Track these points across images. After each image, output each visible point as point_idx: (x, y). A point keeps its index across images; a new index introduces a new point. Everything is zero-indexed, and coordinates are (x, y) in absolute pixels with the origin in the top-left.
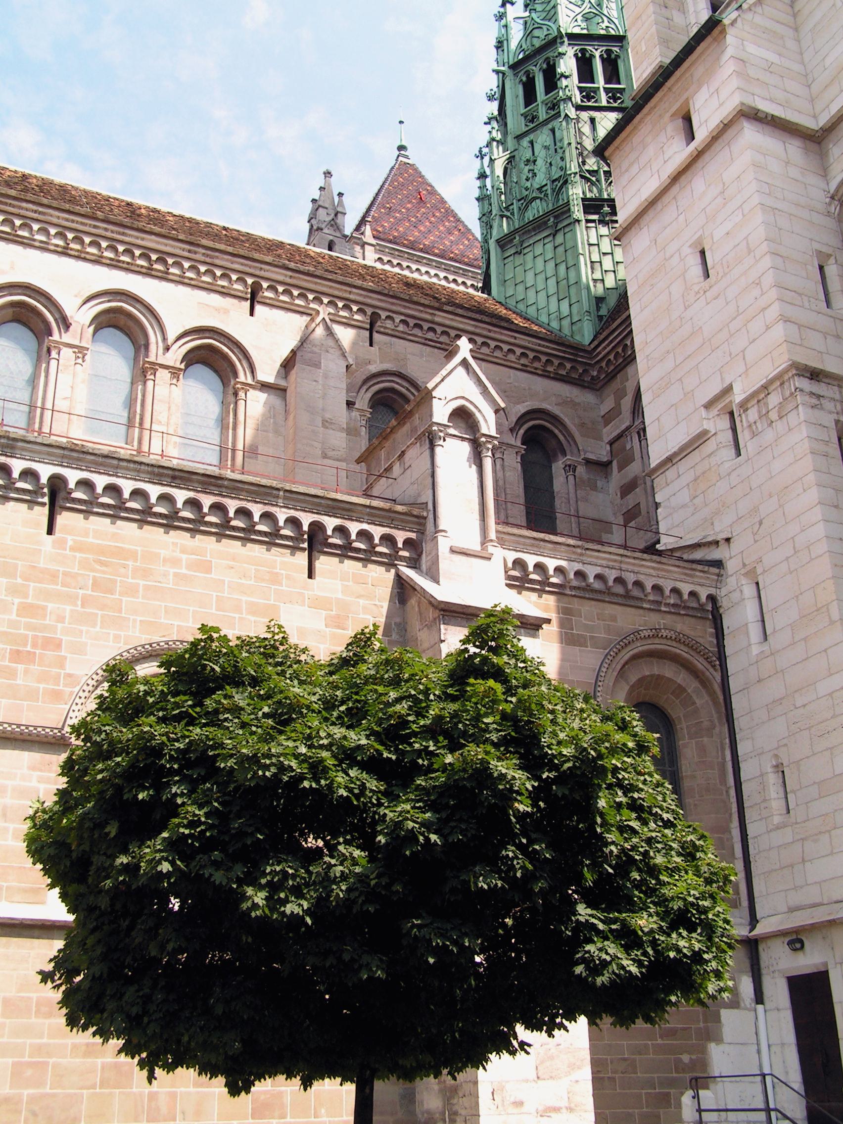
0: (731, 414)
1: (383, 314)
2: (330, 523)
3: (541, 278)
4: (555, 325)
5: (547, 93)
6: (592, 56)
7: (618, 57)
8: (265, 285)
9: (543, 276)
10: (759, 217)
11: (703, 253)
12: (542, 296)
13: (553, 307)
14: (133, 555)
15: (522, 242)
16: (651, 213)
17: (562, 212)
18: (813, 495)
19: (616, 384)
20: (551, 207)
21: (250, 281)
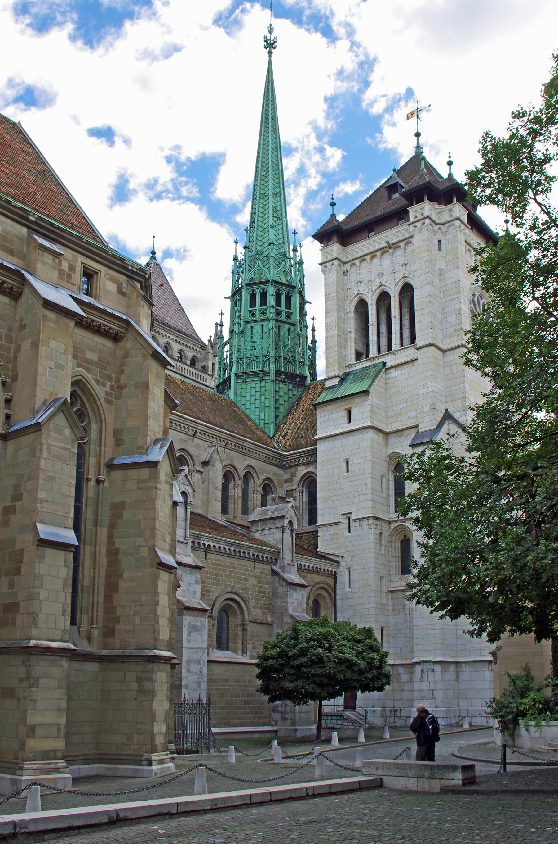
0: (349, 519)
1: (230, 442)
2: (261, 555)
3: (253, 399)
4: (257, 421)
5: (261, 306)
6: (282, 293)
7: (292, 296)
8: (199, 431)
9: (254, 397)
10: (370, 465)
11: (348, 462)
12: (253, 407)
13: (257, 413)
14: (220, 565)
15: (246, 378)
16: (331, 439)
17: (268, 373)
18: (372, 555)
19: (293, 470)
20: (260, 369)
21: (195, 430)
